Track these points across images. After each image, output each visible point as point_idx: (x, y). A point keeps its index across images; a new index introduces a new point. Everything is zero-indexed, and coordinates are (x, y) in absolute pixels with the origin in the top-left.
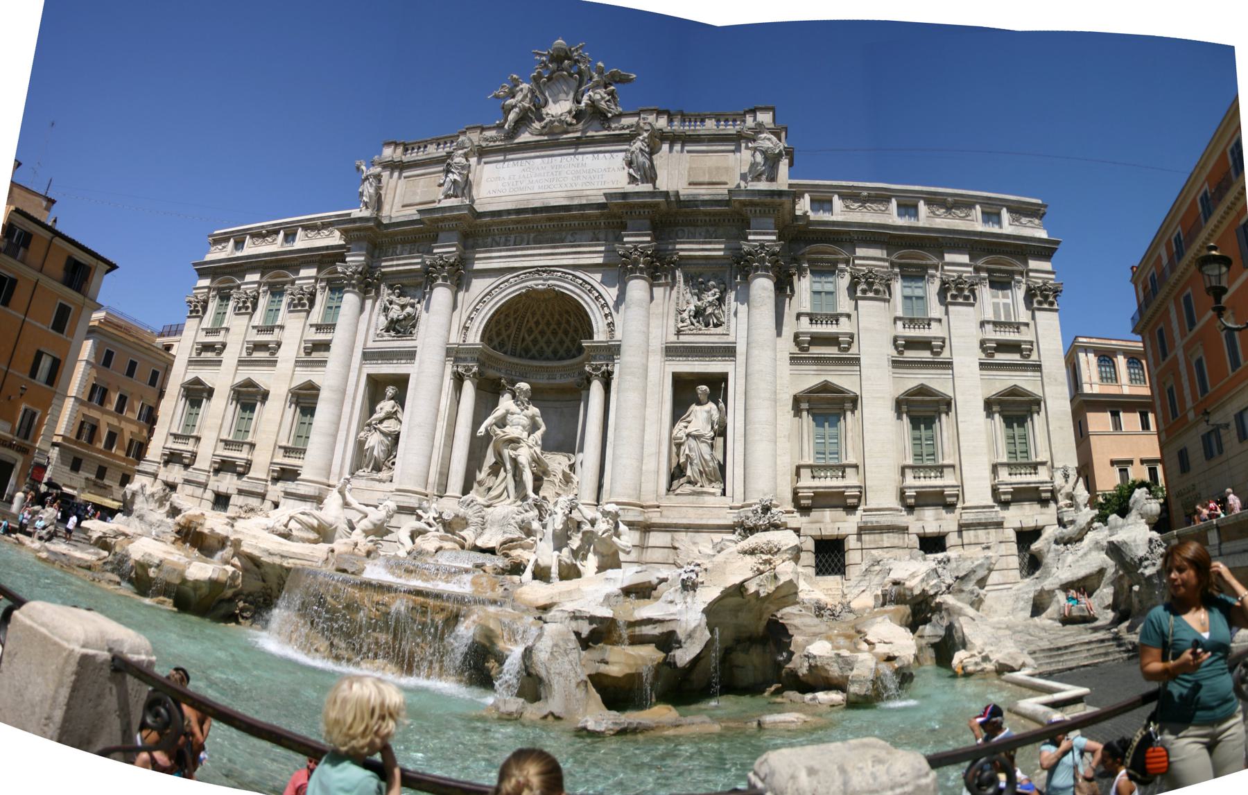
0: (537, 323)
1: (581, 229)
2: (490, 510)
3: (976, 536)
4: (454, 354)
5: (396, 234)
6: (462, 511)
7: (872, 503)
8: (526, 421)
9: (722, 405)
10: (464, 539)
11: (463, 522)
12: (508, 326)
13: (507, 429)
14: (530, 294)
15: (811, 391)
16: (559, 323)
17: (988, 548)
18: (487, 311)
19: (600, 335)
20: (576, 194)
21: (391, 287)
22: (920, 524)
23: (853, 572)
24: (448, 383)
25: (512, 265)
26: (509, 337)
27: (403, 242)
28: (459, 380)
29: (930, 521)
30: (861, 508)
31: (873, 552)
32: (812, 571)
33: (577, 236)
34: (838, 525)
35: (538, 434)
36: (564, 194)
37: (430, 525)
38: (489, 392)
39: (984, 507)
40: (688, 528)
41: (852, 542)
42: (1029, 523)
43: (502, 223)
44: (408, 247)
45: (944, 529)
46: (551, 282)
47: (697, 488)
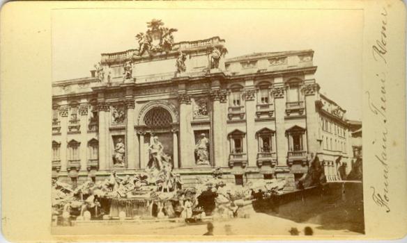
4: (137, 128)
11: (145, 177)
18: (143, 115)
19: (175, 121)
21: (114, 107)
28: (139, 135)
29: (268, 170)
35: (161, 150)
38: (147, 137)
41: (244, 176)
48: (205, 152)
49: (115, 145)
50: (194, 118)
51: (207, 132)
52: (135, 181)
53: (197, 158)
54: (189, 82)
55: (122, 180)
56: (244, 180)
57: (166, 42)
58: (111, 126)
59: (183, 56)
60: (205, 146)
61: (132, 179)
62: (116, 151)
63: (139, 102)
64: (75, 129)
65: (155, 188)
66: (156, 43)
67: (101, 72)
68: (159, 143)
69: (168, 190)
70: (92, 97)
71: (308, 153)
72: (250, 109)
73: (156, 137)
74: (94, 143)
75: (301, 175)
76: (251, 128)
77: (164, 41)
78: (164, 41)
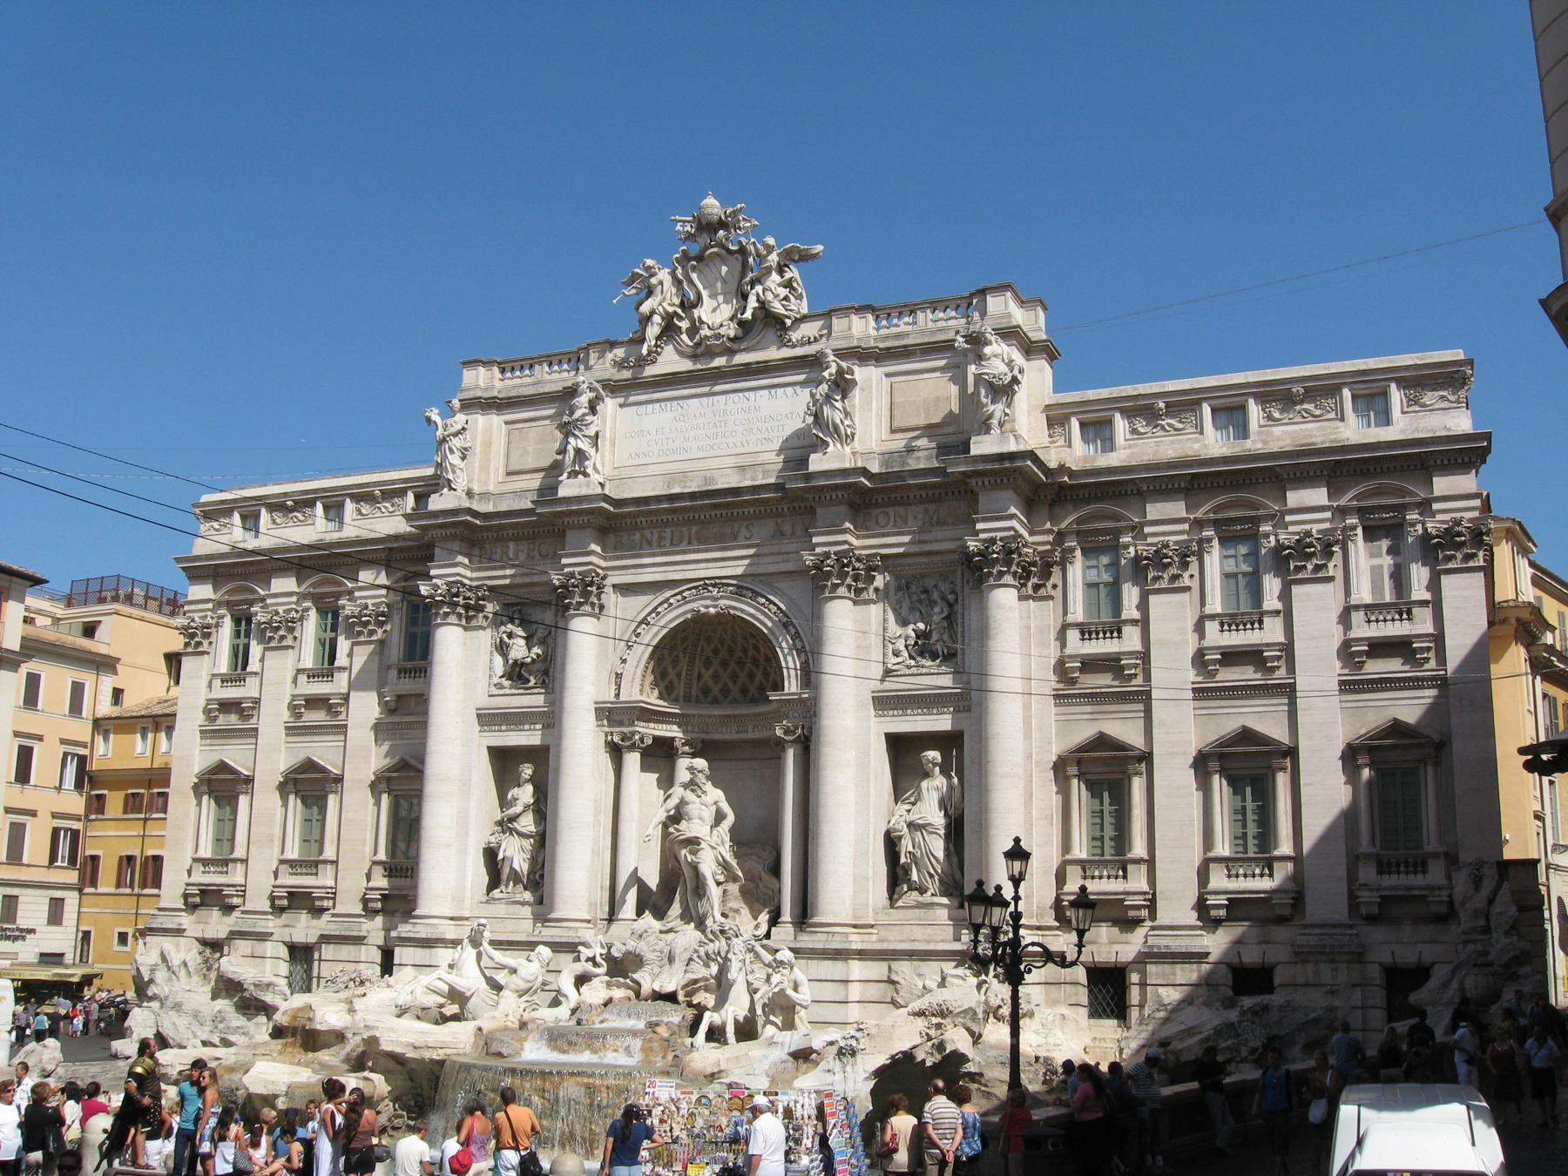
0: (716, 651)
1: (759, 517)
2: (670, 936)
5: (504, 527)
6: (632, 945)
7: (1163, 918)
8: (709, 815)
9: (956, 780)
10: (639, 984)
12: (675, 662)
13: (683, 825)
14: (699, 620)
15: (1081, 749)
16: (745, 650)
17: (1332, 992)
19: (792, 685)
20: (747, 460)
23: (1134, 1014)
24: (606, 760)
25: (671, 577)
26: (679, 675)
27: (518, 539)
28: (616, 752)
30: (1148, 923)
31: (1161, 990)
32: (1084, 1012)
33: (755, 530)
34: (1116, 947)
36: (731, 461)
37: (596, 964)
39: (1334, 926)
40: (912, 955)
42: (1408, 957)
43: (651, 511)
44: (524, 546)
45: (1271, 958)
46: (722, 603)
47: (927, 898)
48: (938, 846)
49: (504, 803)
50: (888, 673)
51: (949, 742)
52: (581, 980)
53: (897, 877)
54: (866, 497)
55: (514, 971)
56: (1134, 995)
57: (763, 304)
58: (484, 701)
59: (840, 372)
60: (938, 819)
61: (569, 969)
62: (506, 825)
63: (626, 589)
64: (317, 712)
65: (675, 1016)
66: (716, 314)
67: (456, 443)
68: (715, 795)
69: (730, 1030)
70: (406, 558)
71: (1452, 860)
72: (1173, 629)
73: (701, 763)
74: (403, 784)
75: (1420, 974)
76: (1179, 729)
77: (752, 303)
78: (752, 303)
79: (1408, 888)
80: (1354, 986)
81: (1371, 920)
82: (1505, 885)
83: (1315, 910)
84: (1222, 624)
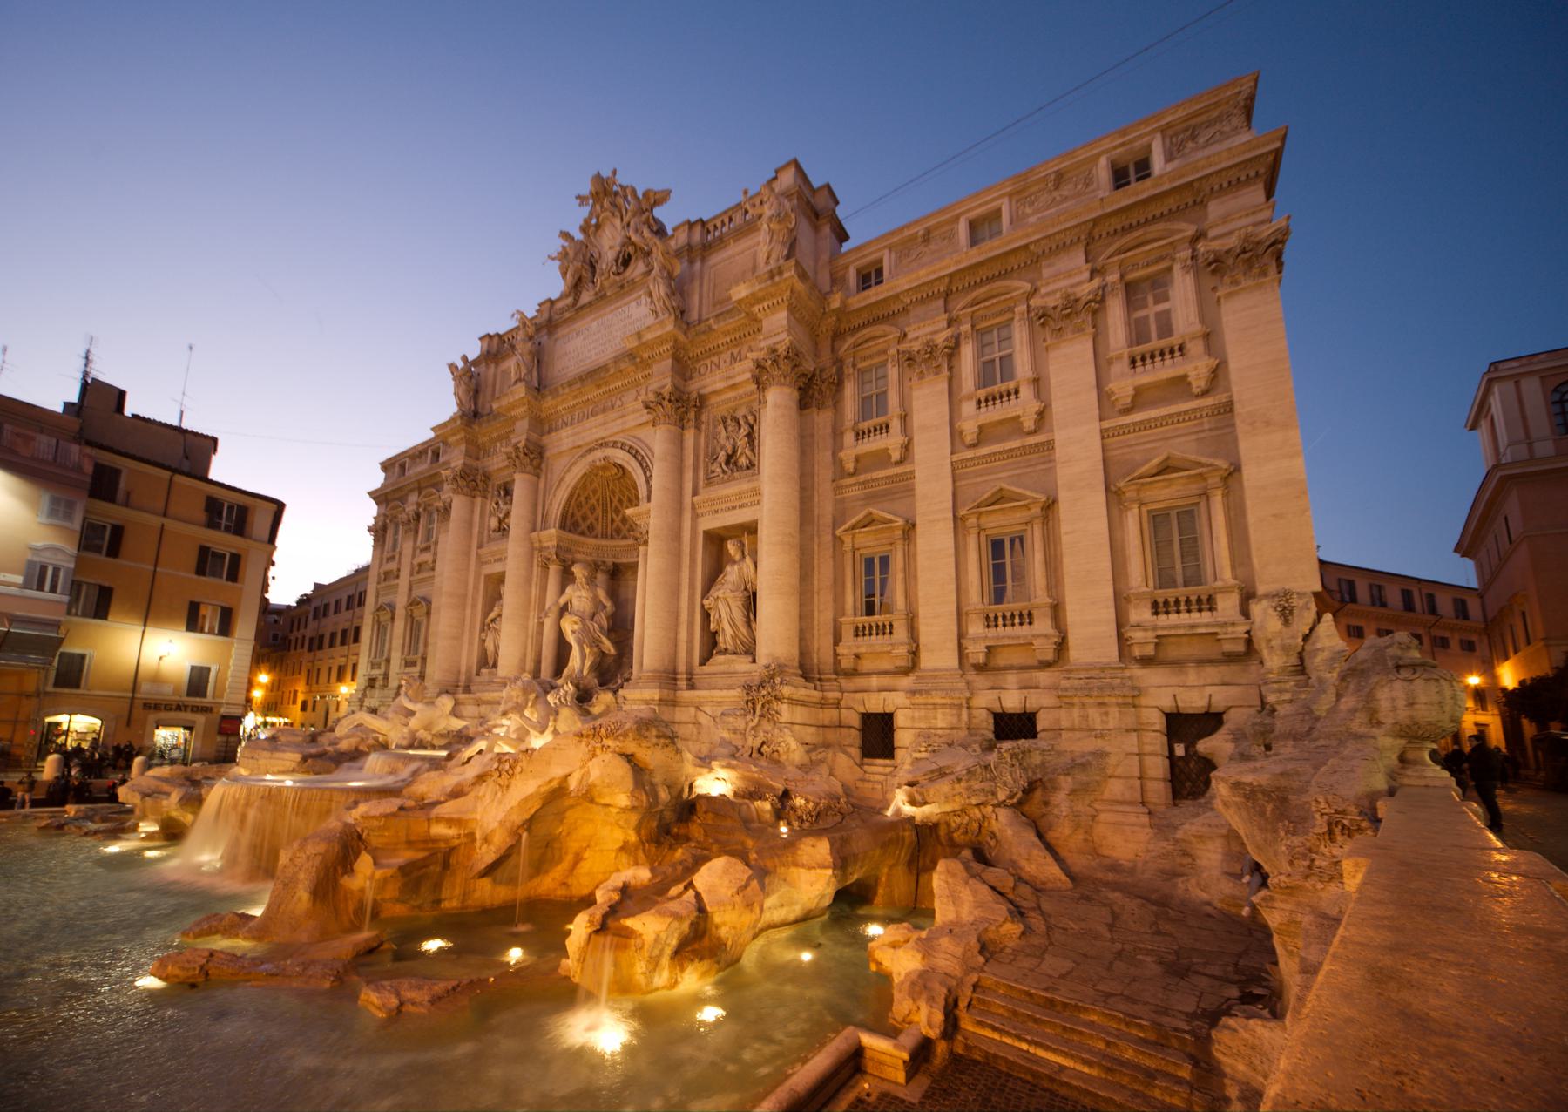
3: (1085, 718)
22: (993, 695)
42: (1194, 701)
45: (1032, 704)
79: (1192, 626)
80: (1128, 731)
81: (1146, 662)
82: (1328, 617)
83: (1078, 653)
84: (979, 402)
